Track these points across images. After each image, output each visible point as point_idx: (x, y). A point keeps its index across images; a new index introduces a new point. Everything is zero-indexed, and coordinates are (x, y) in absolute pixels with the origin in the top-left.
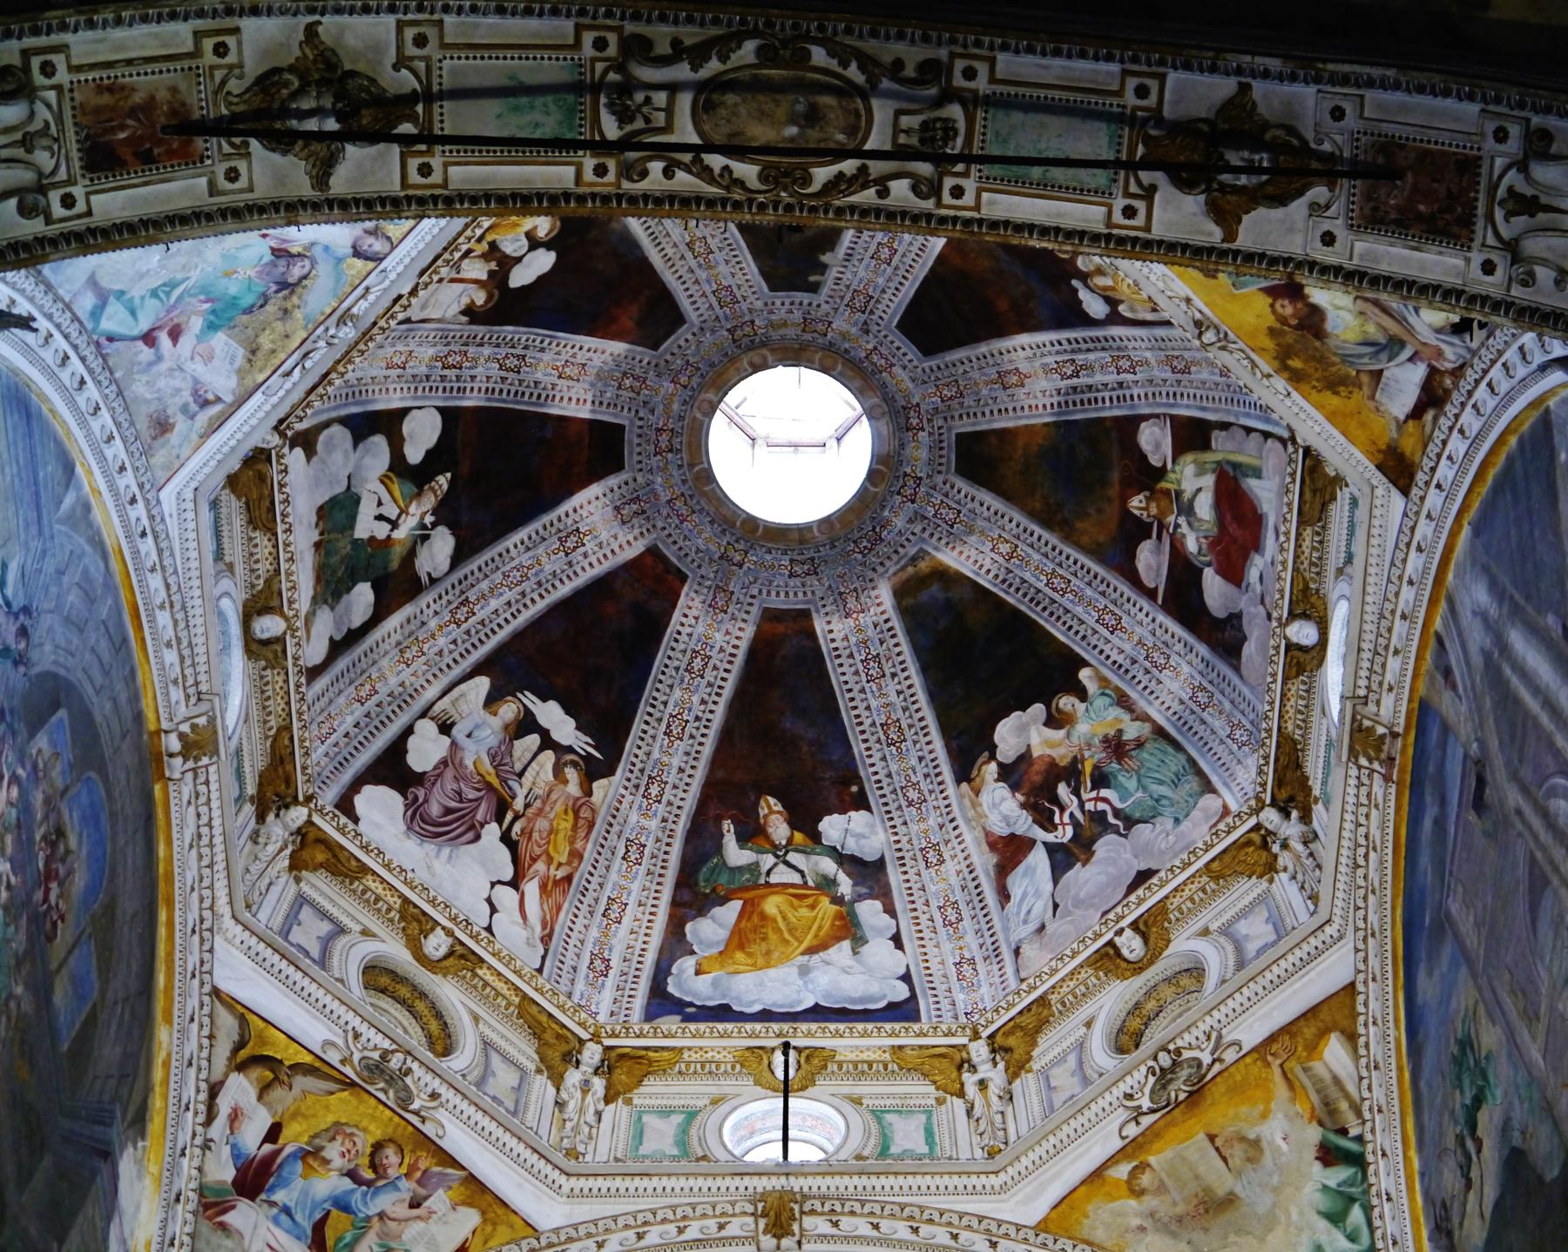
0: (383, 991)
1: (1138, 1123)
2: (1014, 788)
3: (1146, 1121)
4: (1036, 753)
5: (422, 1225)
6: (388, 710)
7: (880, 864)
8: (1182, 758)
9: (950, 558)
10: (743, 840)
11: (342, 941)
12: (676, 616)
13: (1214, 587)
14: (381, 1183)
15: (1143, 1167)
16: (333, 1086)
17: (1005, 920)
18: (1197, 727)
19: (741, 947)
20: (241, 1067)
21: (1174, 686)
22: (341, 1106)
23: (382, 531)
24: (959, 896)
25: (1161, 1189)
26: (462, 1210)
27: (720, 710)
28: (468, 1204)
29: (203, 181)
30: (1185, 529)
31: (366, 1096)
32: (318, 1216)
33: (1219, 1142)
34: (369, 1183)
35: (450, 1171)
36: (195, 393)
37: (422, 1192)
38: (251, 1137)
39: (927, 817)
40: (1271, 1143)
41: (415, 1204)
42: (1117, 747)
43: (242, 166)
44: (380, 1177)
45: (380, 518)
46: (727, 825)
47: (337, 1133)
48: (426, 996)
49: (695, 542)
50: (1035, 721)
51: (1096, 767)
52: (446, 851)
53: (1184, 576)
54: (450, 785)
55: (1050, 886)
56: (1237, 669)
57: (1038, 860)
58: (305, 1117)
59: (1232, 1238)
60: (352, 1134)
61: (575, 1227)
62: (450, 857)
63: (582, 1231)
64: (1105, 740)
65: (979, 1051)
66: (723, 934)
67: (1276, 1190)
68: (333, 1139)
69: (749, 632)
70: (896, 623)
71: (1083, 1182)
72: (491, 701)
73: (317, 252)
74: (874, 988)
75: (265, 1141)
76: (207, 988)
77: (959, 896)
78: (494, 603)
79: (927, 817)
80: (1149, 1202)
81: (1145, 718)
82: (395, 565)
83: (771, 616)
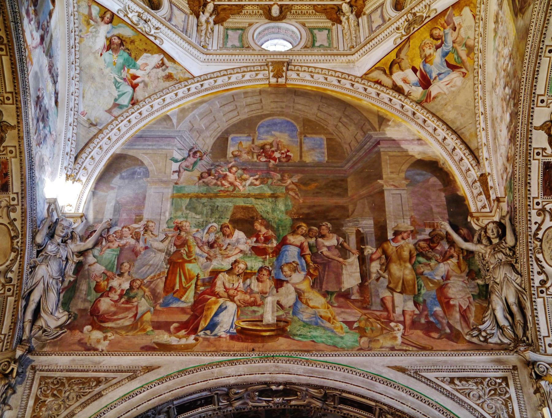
5: (462, 29)
16: (407, 45)
20: (391, 73)
22: (415, 43)
26: (463, 12)
29: (13, 159)
32: (445, 64)
34: (442, 43)
35: (448, 13)
36: (158, 67)
37: (451, 25)
38: (413, 78)
41: (454, 29)
43: (9, 149)
44: (441, 39)
58: (414, 57)
68: (424, 50)
73: (109, 36)
75: (416, 74)
76: (360, 80)
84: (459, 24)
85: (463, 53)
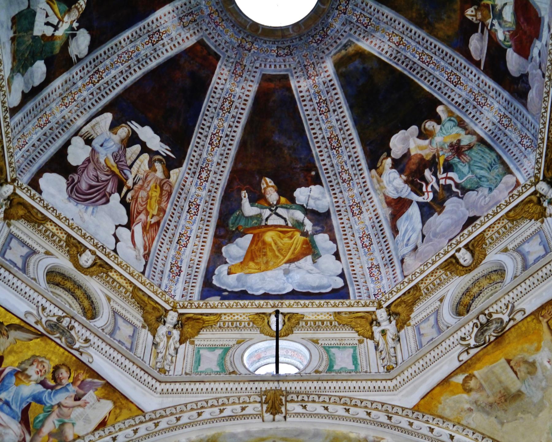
0: (58, 285)
1: (468, 353)
2: (401, 172)
3: (473, 352)
4: (413, 153)
5: (80, 410)
6: (56, 132)
7: (328, 214)
8: (494, 155)
9: (365, 45)
10: (253, 201)
11: (34, 258)
12: (214, 79)
13: (513, 61)
14: (59, 387)
15: (471, 377)
16: (31, 336)
17: (396, 244)
18: (502, 138)
19: (252, 259)
21: (490, 115)
22: (36, 346)
23: (49, 31)
24: (371, 231)
25: (481, 388)
26: (103, 401)
27: (239, 130)
28: (106, 398)
30: (497, 26)
31: (50, 341)
32: (24, 405)
33: (512, 363)
34: (52, 388)
35: (96, 380)
37: (81, 392)
39: (352, 188)
40: (541, 364)
41: (77, 398)
42: (457, 149)
44: (58, 384)
45: (47, 24)
46: (244, 193)
47: (34, 361)
48: (81, 287)
49: (223, 38)
50: (412, 135)
51: (446, 160)
52: (90, 209)
53: (496, 53)
54: (92, 173)
55: (420, 226)
56: (525, 105)
57: (414, 211)
58: (16, 353)
59: (520, 415)
60: (42, 362)
61: (165, 410)
62: (93, 212)
63: (168, 412)
64: (451, 145)
65: (382, 315)
66: (243, 253)
67: (544, 389)
68: (32, 364)
69: (254, 88)
70: (335, 82)
71: (438, 385)
72: (113, 127)
74: (325, 281)
77: (371, 231)
78: (113, 72)
79: (352, 188)
80: (474, 395)
81: (473, 133)
82: (57, 50)
83: (266, 79)
84: (86, 403)
85: (50, 426)
